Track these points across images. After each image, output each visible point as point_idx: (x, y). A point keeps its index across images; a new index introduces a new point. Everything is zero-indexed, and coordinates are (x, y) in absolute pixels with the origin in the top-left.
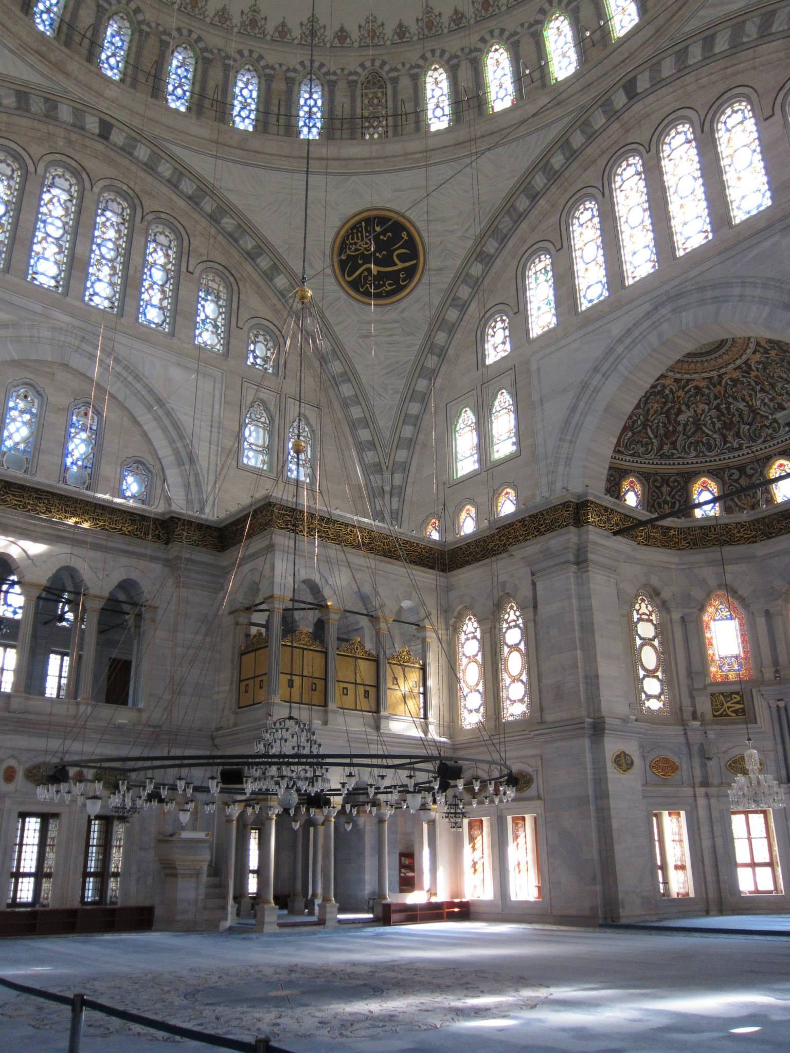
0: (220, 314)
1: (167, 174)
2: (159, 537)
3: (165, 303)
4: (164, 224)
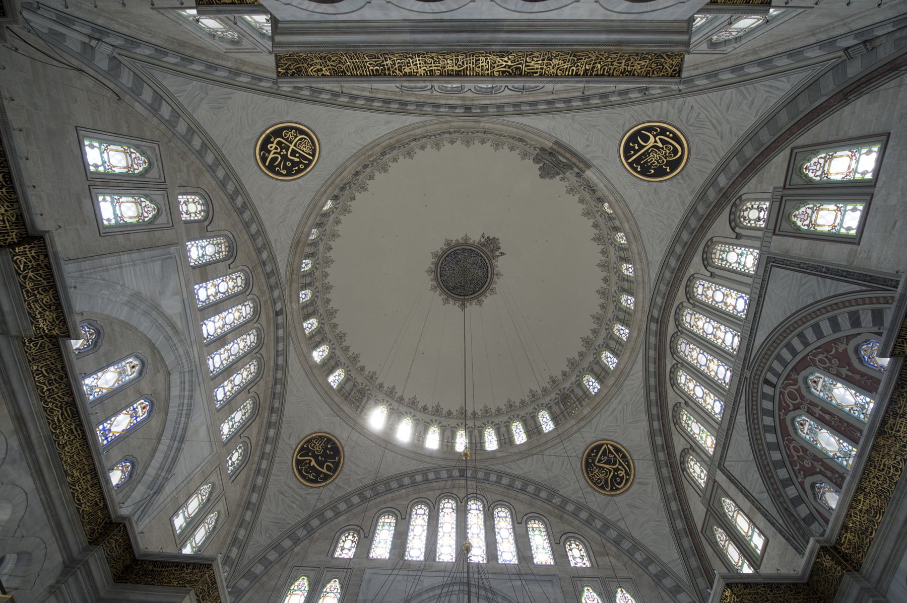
1: (280, 349)
3: (228, 394)
4: (258, 364)
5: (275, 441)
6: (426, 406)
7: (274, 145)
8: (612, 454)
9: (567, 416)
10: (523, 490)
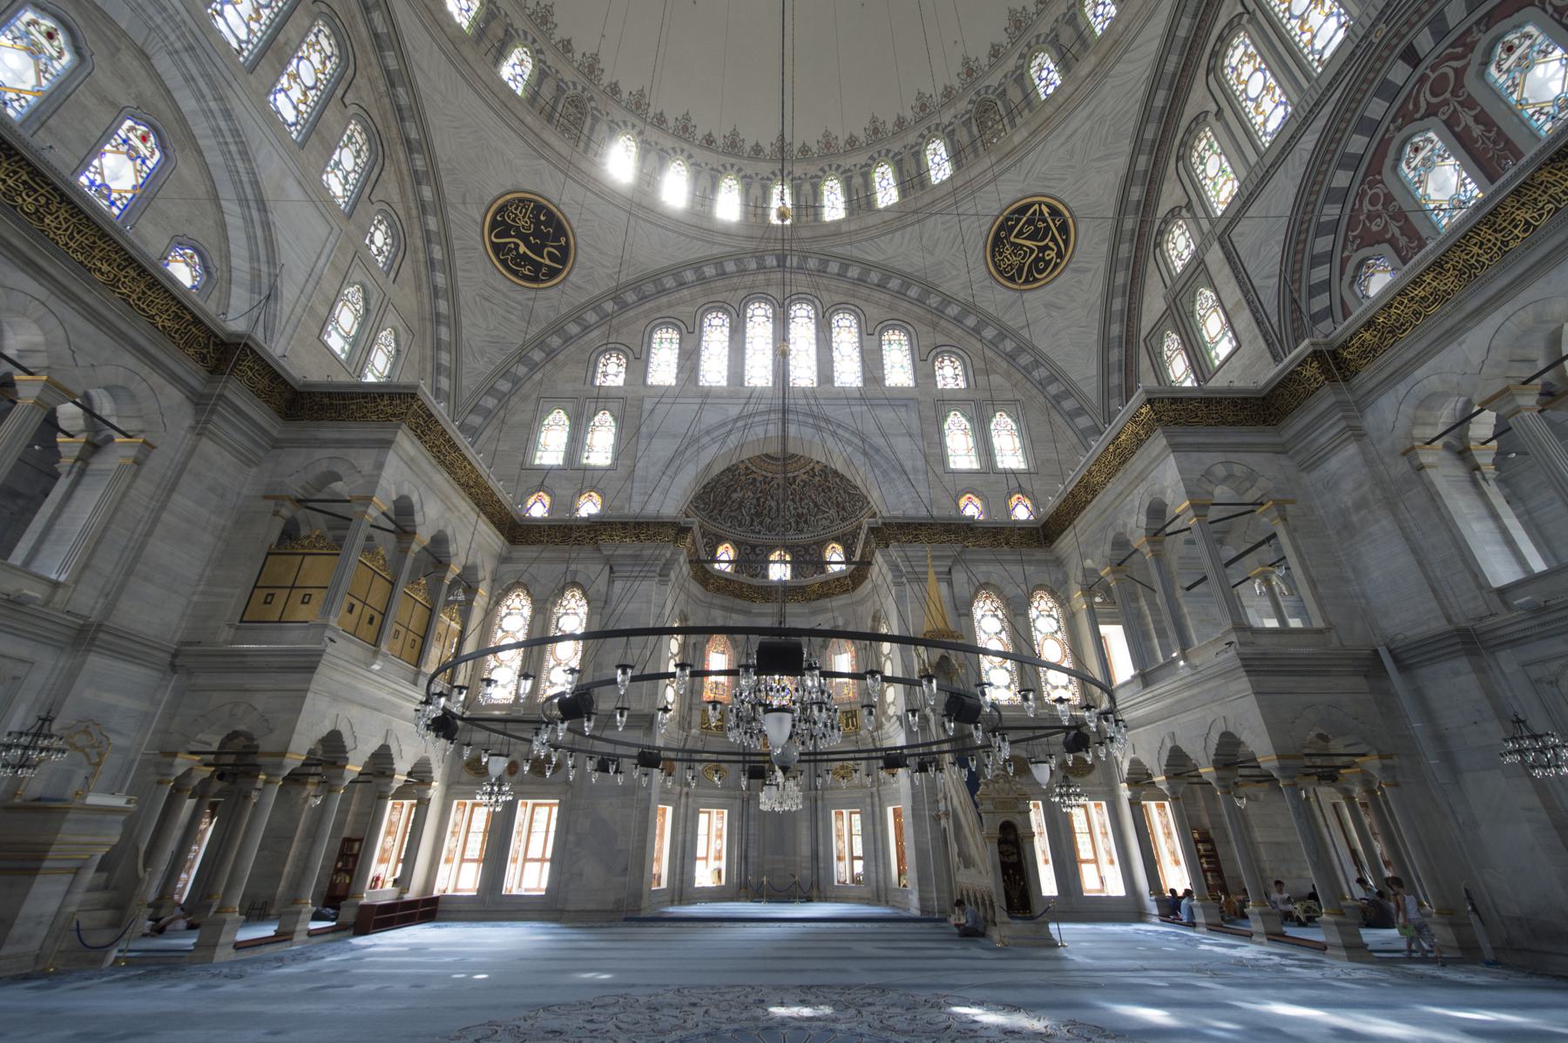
0: (355, 171)
2: (203, 358)
5: (440, 207)
6: (710, 135)
8: (1045, 221)
9: (981, 149)
10: (881, 286)
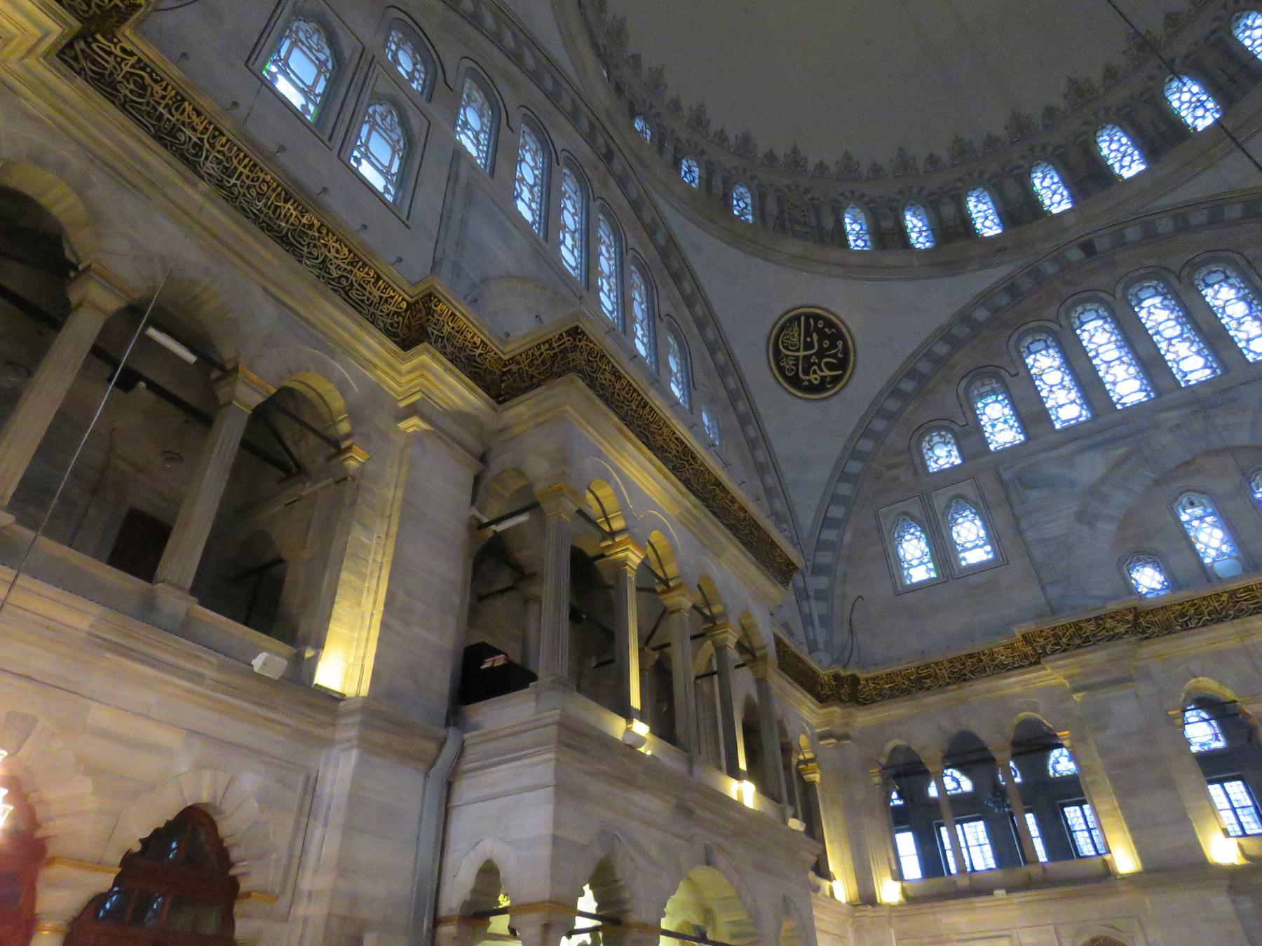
7: (812, 377)
